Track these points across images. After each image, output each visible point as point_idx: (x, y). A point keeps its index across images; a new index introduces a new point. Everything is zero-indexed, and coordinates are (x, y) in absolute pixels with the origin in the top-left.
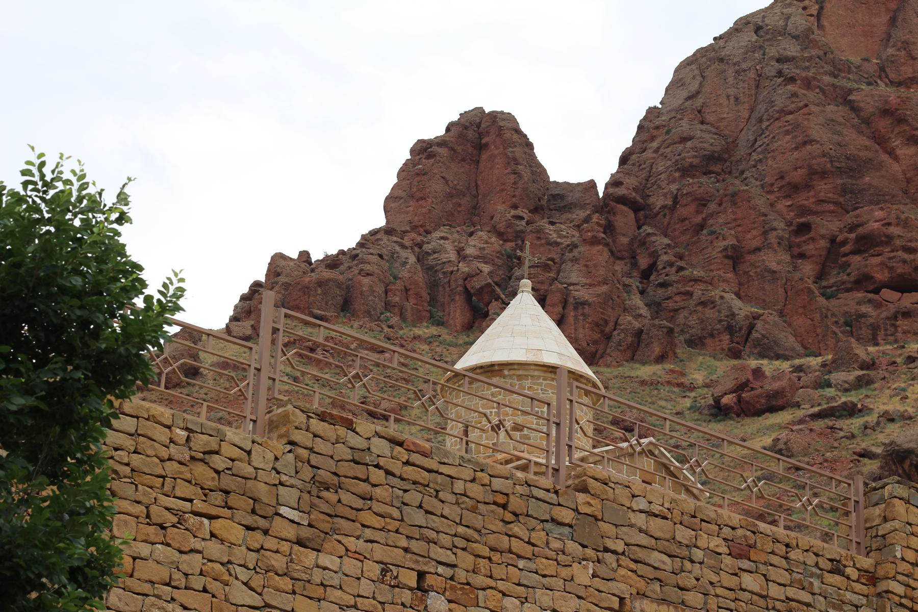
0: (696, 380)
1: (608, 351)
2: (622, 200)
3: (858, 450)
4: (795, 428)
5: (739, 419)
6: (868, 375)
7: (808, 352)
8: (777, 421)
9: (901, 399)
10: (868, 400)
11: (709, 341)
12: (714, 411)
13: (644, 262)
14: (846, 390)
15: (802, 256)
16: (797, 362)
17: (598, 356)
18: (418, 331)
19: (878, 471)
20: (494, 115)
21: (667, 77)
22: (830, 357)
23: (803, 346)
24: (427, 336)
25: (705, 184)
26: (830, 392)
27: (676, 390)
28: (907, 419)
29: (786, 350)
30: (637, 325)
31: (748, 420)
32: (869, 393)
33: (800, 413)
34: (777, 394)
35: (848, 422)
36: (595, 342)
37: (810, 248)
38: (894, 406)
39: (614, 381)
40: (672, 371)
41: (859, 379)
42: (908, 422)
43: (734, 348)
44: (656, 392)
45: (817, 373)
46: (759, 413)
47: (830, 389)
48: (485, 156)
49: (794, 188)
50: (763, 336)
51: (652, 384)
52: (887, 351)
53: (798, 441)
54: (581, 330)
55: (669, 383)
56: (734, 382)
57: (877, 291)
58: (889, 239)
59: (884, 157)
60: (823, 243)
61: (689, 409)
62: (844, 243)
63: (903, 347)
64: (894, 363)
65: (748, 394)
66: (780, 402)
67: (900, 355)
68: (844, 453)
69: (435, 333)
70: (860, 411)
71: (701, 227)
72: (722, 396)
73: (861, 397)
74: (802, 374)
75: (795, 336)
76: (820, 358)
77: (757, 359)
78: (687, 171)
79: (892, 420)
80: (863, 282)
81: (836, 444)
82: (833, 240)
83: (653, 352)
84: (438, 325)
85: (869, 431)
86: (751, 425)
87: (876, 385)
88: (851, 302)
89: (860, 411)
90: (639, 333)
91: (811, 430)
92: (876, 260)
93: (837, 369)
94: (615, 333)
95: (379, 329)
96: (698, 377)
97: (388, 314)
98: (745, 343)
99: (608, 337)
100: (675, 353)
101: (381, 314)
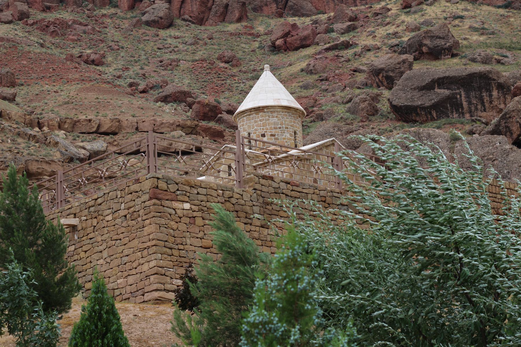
0: (260, 31)
1: (210, 17)
3: (353, 68)
4: (317, 57)
5: (286, 53)
6: (354, 24)
7: (319, 12)
8: (307, 53)
9: (373, 37)
10: (355, 39)
11: (265, 8)
12: (272, 48)
14: (343, 33)
16: (314, 17)
17: (205, 20)
18: (104, 12)
19: (365, 80)
22: (332, 14)
23: (316, 8)
24: (109, 14)
26: (334, 35)
27: (250, 37)
28: (377, 49)
29: (308, 11)
31: (291, 53)
32: (355, 34)
33: (319, 48)
34: (306, 38)
35: (346, 52)
36: (203, 12)
38: (370, 42)
39: (215, 34)
40: (246, 27)
41: (349, 27)
42: (377, 51)
43: (279, 11)
44: (239, 39)
45: (326, 25)
46: (297, 49)
47: (334, 33)
50: (294, 4)
51: (236, 35)
52: (362, 10)
53: (320, 64)
54: (195, 6)
55: (245, 33)
56: (282, 32)
61: (258, 48)
63: (371, 7)
64: (367, 16)
65: (290, 39)
66: (308, 42)
67: (370, 12)
68: (345, 70)
69: (114, 12)
70: (351, 45)
72: (276, 40)
73: (351, 37)
74: (317, 25)
75: (311, 3)
76: (326, 15)
77: (292, 17)
79: (369, 50)
81: (340, 66)
83: (235, 16)
84: (115, 7)
85: (357, 57)
86: (293, 56)
87: (358, 30)
89: (351, 45)
91: (326, 58)
93: (337, 22)
94: (214, 6)
95: (82, 11)
96: (261, 29)
97: (87, 3)
98: (285, 8)
100: (247, 16)
101: (83, 3)
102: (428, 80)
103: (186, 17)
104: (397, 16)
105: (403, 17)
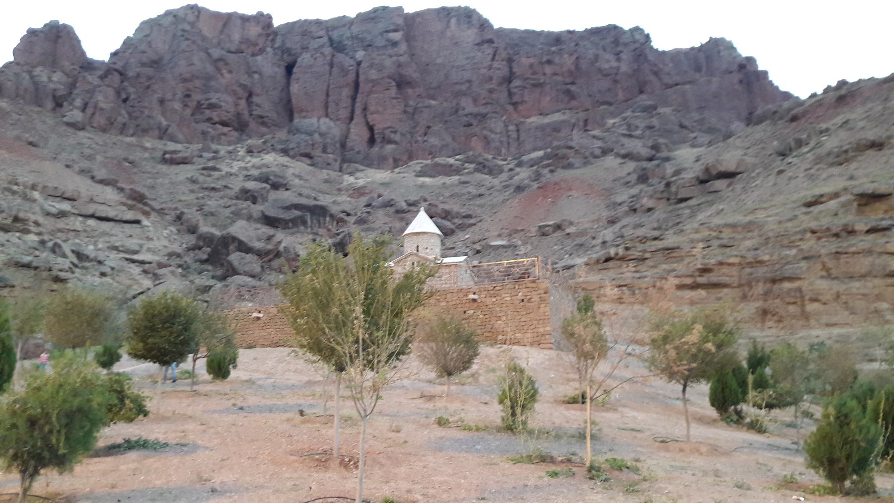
2: (116, 70)
13: (124, 96)
15: (186, 106)
20: (65, 26)
21: (137, 25)
25: (150, 71)
30: (124, 121)
34: (185, 158)
37: (189, 104)
41: (213, 156)
46: (179, 163)
48: (60, 41)
49: (185, 80)
57: (215, 124)
58: (220, 107)
59: (219, 76)
60: (195, 103)
62: (203, 104)
66: (187, 161)
71: (148, 87)
78: (143, 65)
80: (209, 120)
82: (199, 102)
86: (175, 169)
88: (205, 126)
90: (124, 124)
92: (216, 113)
96: (148, 145)
99: (112, 124)
102: (289, 204)
103: (95, 125)
104: (244, 157)
105: (249, 158)
